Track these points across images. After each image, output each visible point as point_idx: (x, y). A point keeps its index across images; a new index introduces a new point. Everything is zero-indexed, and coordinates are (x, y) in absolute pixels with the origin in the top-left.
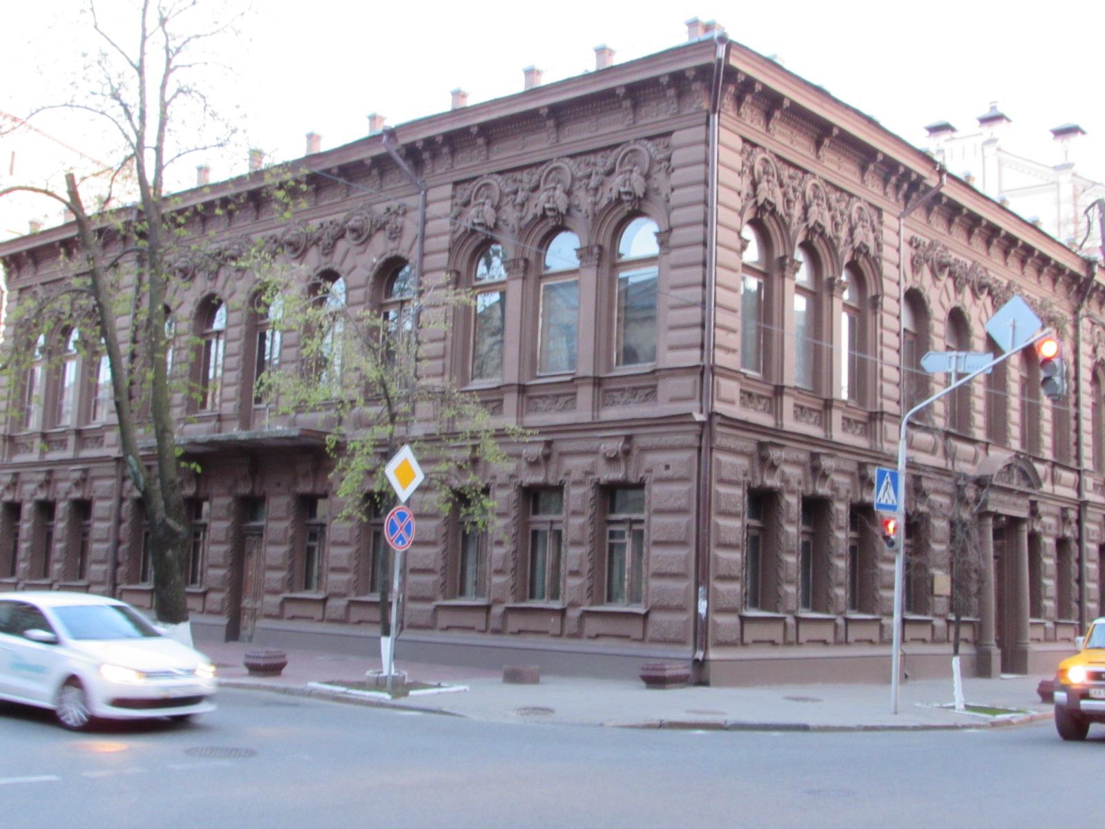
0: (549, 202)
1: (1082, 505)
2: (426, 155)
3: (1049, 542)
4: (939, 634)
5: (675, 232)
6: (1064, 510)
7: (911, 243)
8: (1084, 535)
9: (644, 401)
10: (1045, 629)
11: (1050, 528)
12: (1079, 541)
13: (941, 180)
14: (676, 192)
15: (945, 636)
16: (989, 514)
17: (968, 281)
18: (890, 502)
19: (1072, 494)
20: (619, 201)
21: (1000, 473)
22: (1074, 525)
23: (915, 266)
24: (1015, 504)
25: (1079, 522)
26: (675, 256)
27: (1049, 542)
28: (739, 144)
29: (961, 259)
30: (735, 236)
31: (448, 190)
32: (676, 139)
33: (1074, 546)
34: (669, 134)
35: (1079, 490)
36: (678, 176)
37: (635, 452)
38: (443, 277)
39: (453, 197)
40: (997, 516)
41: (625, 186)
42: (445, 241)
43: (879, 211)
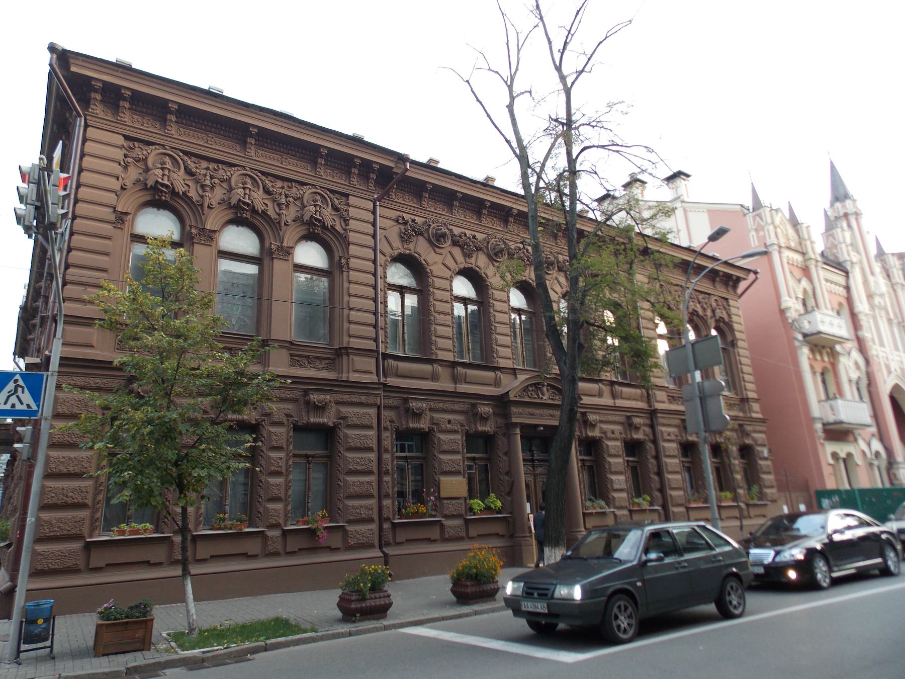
1: (652, 414)
3: (614, 445)
4: (449, 533)
6: (628, 418)
7: (397, 221)
8: (659, 436)
10: (615, 516)
11: (613, 433)
12: (655, 441)
13: (405, 166)
15: (463, 534)
16: (516, 424)
17: (479, 249)
18: (19, 407)
19: (642, 405)
21: (525, 389)
22: (647, 430)
23: (405, 238)
24: (551, 416)
25: (652, 426)
27: (614, 445)
28: (120, 140)
29: (468, 233)
30: (111, 210)
33: (650, 446)
35: (649, 401)
40: (523, 426)
43: (347, 196)
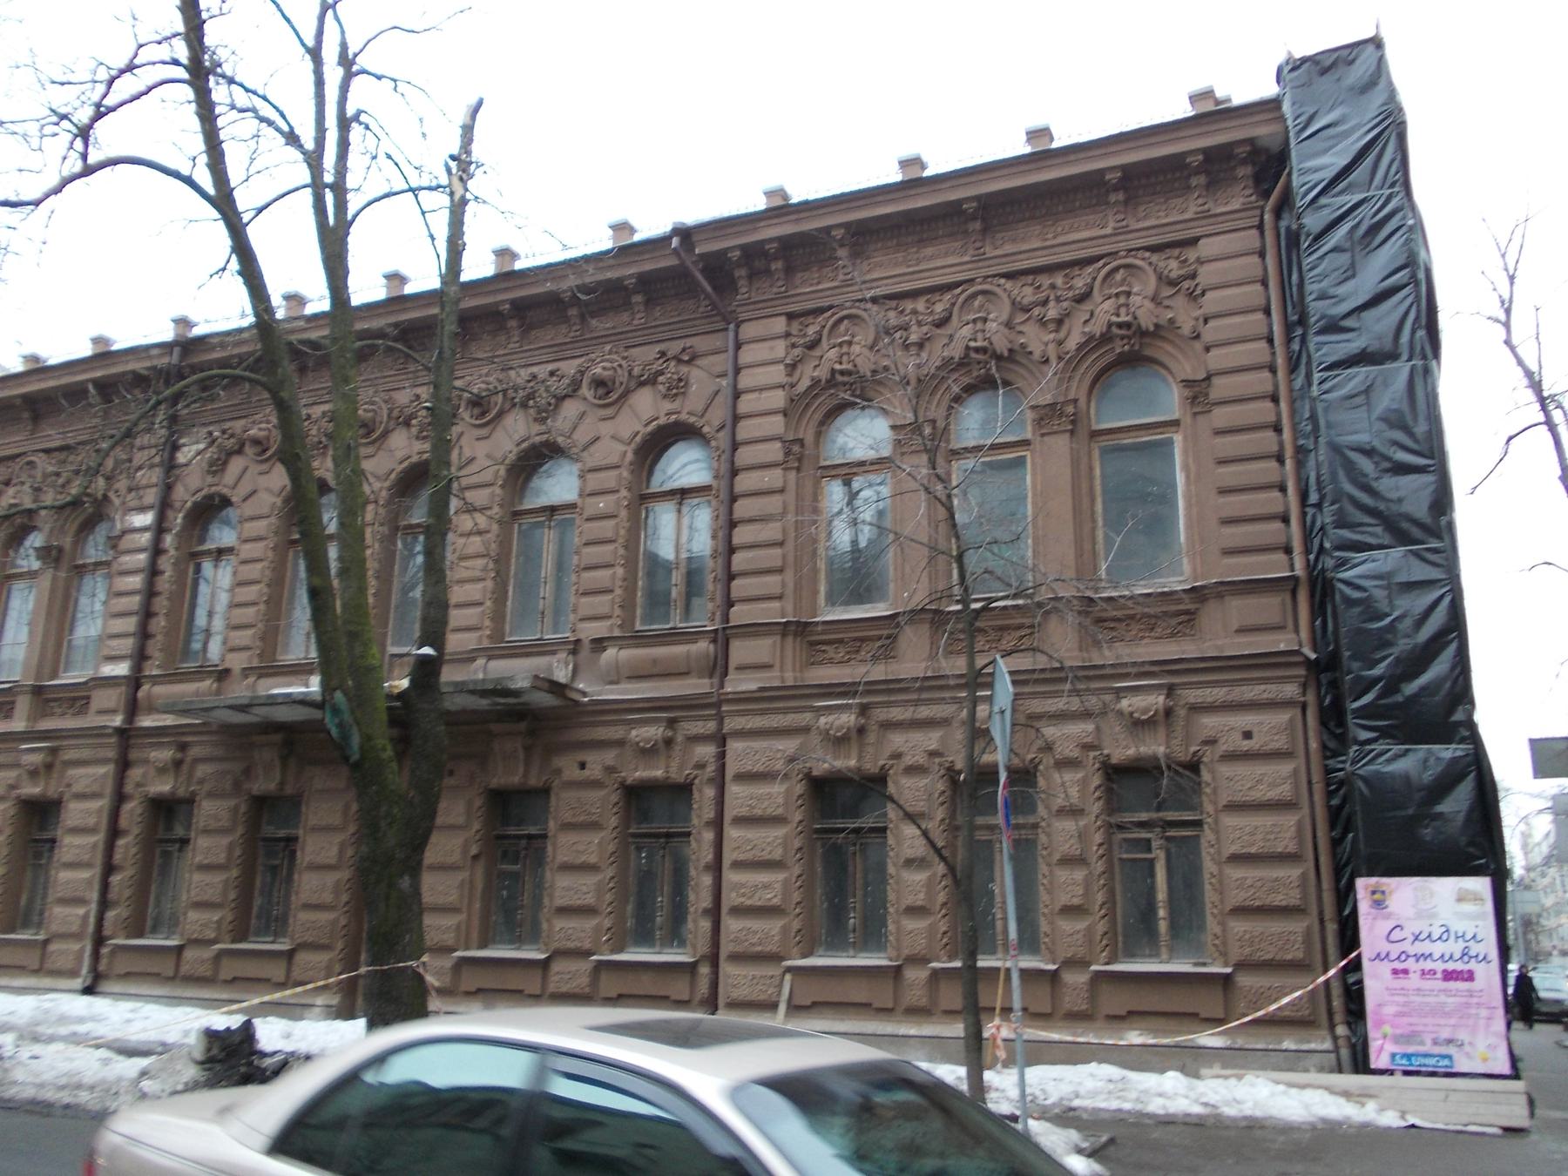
0: (975, 340)
2: (741, 272)
5: (1216, 381)
9: (1172, 635)
14: (1212, 324)
20: (1106, 338)
26: (1222, 416)
31: (780, 325)
32: (1207, 247)
34: (1193, 242)
36: (1212, 302)
37: (1182, 712)
38: (774, 451)
39: (788, 335)
41: (1118, 315)
42: (778, 399)
